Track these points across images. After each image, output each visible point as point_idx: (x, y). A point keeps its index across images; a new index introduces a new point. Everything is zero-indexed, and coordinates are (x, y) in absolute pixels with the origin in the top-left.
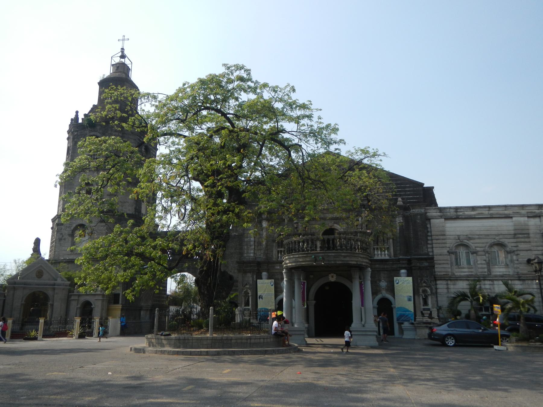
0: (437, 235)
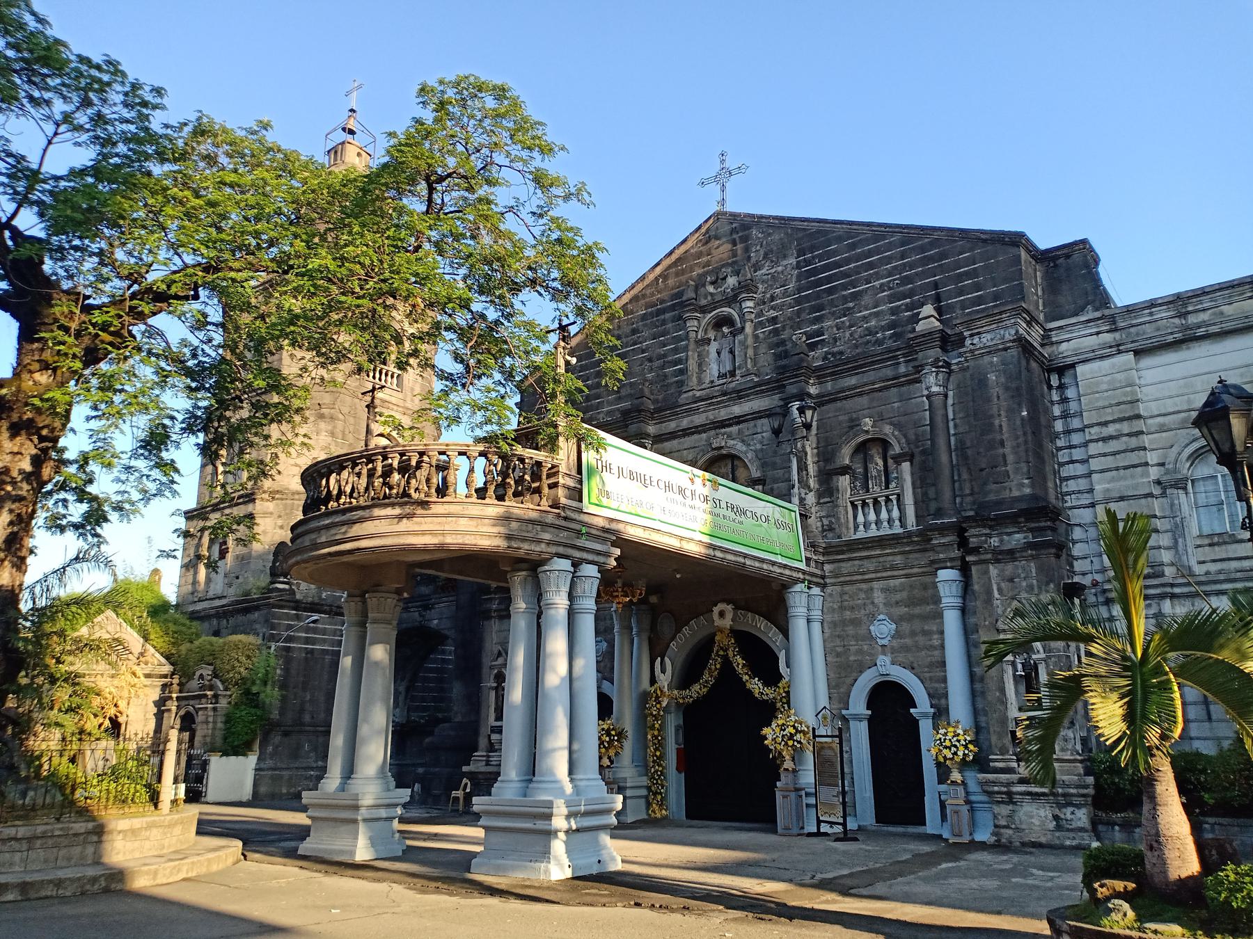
0: (1105, 424)
